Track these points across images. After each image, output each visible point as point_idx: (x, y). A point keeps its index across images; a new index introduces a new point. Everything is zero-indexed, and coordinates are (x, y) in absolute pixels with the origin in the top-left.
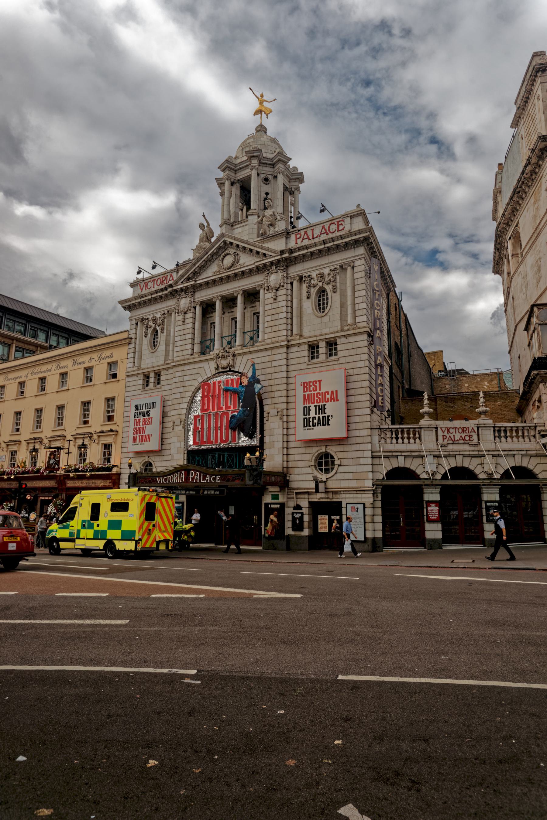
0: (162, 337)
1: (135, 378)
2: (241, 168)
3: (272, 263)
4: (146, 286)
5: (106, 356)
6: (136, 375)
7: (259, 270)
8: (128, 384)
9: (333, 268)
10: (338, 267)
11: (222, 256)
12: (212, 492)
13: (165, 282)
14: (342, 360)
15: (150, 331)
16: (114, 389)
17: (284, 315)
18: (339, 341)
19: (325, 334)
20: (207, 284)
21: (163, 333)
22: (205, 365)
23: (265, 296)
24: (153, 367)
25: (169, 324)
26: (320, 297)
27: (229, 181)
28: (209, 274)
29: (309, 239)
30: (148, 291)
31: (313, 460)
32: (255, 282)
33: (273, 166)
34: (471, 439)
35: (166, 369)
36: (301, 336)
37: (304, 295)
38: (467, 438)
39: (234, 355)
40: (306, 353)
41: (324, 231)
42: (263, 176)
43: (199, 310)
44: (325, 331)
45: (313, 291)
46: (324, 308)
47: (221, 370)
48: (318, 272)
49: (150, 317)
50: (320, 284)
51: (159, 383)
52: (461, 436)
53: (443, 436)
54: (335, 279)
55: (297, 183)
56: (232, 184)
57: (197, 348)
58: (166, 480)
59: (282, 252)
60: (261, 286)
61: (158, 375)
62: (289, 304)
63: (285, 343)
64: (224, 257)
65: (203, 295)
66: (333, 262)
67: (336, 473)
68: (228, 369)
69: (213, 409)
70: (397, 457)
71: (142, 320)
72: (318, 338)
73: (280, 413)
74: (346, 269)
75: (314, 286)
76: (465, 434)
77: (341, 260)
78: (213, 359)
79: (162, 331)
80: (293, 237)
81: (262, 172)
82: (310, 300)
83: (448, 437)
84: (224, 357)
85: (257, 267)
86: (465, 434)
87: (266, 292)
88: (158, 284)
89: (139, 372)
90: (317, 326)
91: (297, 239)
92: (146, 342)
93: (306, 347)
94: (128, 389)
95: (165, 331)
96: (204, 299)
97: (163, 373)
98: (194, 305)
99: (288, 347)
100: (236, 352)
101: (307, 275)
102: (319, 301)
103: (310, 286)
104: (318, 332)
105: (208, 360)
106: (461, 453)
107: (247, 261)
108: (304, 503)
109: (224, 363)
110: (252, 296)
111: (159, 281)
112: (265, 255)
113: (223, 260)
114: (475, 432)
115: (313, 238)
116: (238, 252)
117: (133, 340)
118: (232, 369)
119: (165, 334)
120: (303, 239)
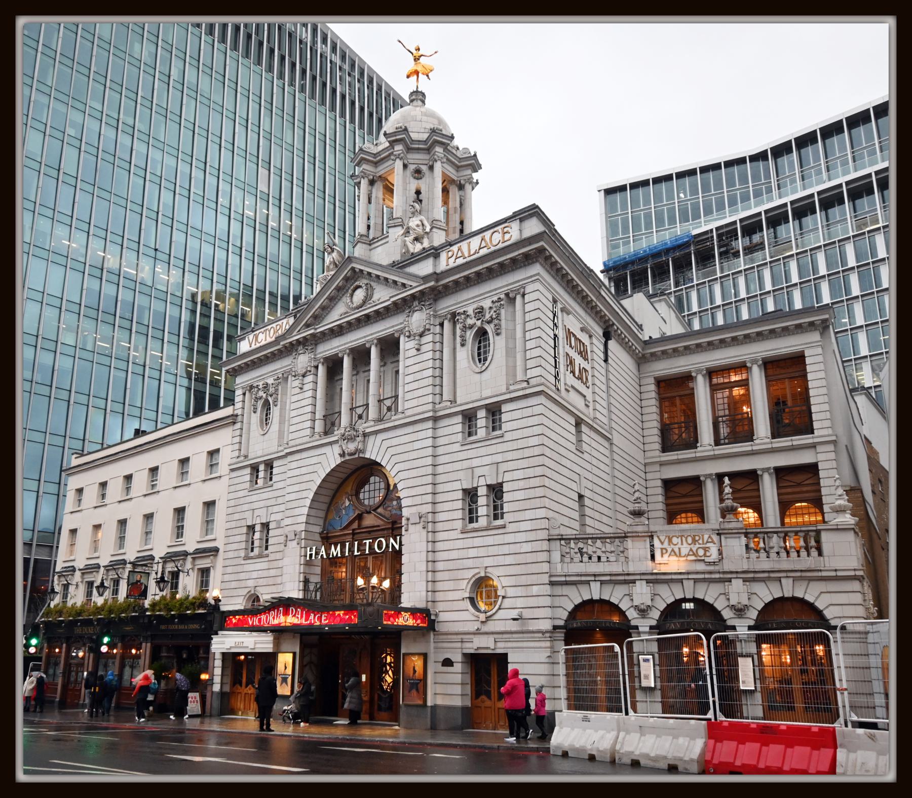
0: (275, 412)
2: (382, 159)
3: (413, 297)
9: (495, 298)
10: (503, 296)
11: (350, 291)
14: (508, 436)
15: (260, 404)
16: (216, 491)
17: (430, 372)
18: (504, 408)
20: (339, 331)
22: (327, 450)
23: (406, 345)
25: (285, 393)
26: (480, 343)
27: (366, 179)
28: (335, 317)
31: (468, 590)
32: (393, 327)
33: (428, 150)
34: (708, 554)
36: (453, 401)
37: (458, 340)
38: (701, 552)
39: (365, 435)
42: (412, 167)
43: (322, 370)
45: (470, 335)
46: (485, 359)
48: (475, 306)
49: (261, 383)
50: (479, 323)
51: (271, 479)
52: (691, 550)
53: (662, 549)
54: (499, 314)
55: (469, 172)
56: (372, 183)
57: (319, 426)
60: (401, 331)
61: (269, 465)
62: (438, 355)
63: (430, 414)
64: (354, 291)
66: (496, 290)
67: (499, 609)
70: (588, 582)
71: (252, 387)
73: (423, 519)
74: (515, 298)
75: (471, 327)
76: (698, 546)
79: (275, 402)
80: (443, 256)
81: (412, 161)
82: (465, 348)
83: (669, 550)
84: (352, 439)
85: (395, 303)
86: (698, 546)
87: (407, 339)
90: (475, 385)
92: (255, 418)
93: (459, 419)
95: (279, 403)
96: (328, 354)
98: (316, 364)
99: (435, 419)
100: (368, 430)
101: (461, 311)
102: (479, 348)
103: (465, 327)
105: (331, 443)
106: (690, 576)
107: (383, 296)
109: (352, 447)
112: (404, 285)
113: (352, 295)
114: (713, 542)
116: (372, 283)
117: (239, 418)
119: (279, 406)
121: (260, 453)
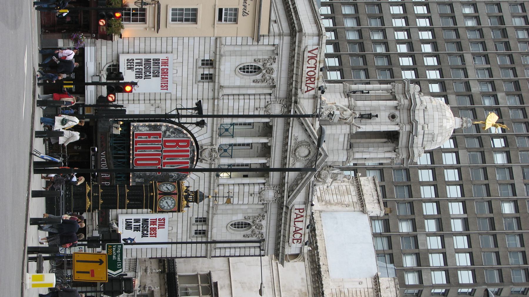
1: (213, 49)
4: (312, 58)
5: (247, 5)
6: (215, 53)
7: (282, 184)
8: (208, 40)
12: (93, 164)
13: (309, 82)
19: (211, 232)
21: (254, 81)
24: (219, 75)
29: (295, 219)
30: (306, 59)
35: (214, 90)
40: (200, 216)
41: (297, 229)
44: (214, 231)
45: (250, 221)
47: (200, 151)
49: (275, 66)
58: (103, 161)
59: (287, 207)
65: (278, 125)
68: (199, 157)
69: (165, 151)
72: (210, 227)
77: (268, 241)
78: (212, 144)
88: (309, 74)
89: (218, 56)
91: (299, 209)
94: (202, 41)
95: (254, 84)
97: (211, 84)
104: (215, 224)
109: (206, 154)
110: (264, 171)
111: (312, 73)
115: (295, 222)
118: (199, 160)
120: (297, 214)
121: (222, 68)
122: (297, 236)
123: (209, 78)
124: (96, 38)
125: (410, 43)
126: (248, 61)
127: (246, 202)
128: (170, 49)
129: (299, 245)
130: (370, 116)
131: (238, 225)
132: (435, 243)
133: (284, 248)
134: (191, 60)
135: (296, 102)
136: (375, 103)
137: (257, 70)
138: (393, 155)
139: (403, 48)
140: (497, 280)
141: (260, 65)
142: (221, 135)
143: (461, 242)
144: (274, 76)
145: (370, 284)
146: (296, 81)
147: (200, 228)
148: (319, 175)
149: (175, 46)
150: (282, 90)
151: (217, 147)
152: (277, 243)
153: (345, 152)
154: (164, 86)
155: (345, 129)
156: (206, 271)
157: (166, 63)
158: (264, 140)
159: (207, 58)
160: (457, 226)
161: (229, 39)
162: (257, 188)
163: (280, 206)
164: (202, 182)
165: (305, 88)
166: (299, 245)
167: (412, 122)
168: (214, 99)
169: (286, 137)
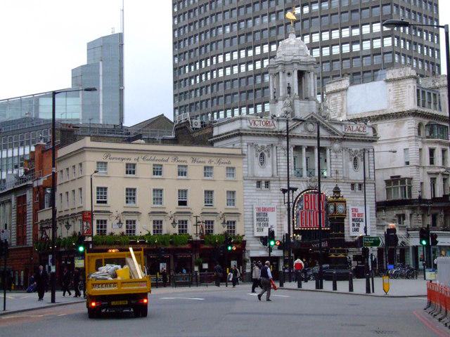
1: (250, 181)
7: (330, 139)
30: (256, 126)
35: (274, 181)
44: (359, 179)
45: (353, 158)
78: (307, 181)
94: (245, 188)
97: (271, 182)
104: (355, 179)
108: (351, 256)
112: (334, 133)
121: (261, 176)
122: (361, 129)
123: (267, 183)
124: (245, 250)
125: (248, 63)
126: (257, 161)
127: (341, 160)
128: (251, 207)
129: (367, 128)
130: (289, 88)
131: (355, 165)
132: (366, 45)
133: (368, 137)
134: (257, 194)
135: (281, 132)
136: (281, 85)
137: (262, 155)
138: (312, 74)
139: (251, 67)
140: (389, 7)
141: (259, 154)
142: (301, 176)
143: (366, 29)
144: (265, 145)
145: (390, 85)
146: (269, 132)
147: (357, 187)
148: (324, 117)
149: (248, 204)
150: (274, 140)
151: (309, 178)
152: (366, 141)
153: (311, 102)
154: (272, 210)
155: (297, 103)
156: (384, 183)
157: (259, 209)
158: (304, 150)
159: (255, 185)
160: (356, 32)
161: (244, 172)
162: (333, 154)
163: (343, 140)
164: (329, 187)
165: (272, 127)
166: (367, 128)
167: (292, 63)
168: (279, 180)
169: (302, 137)
